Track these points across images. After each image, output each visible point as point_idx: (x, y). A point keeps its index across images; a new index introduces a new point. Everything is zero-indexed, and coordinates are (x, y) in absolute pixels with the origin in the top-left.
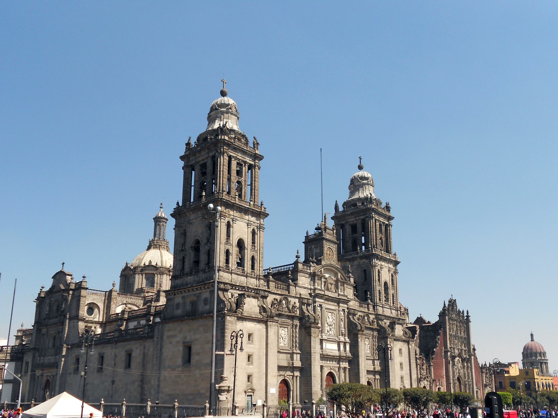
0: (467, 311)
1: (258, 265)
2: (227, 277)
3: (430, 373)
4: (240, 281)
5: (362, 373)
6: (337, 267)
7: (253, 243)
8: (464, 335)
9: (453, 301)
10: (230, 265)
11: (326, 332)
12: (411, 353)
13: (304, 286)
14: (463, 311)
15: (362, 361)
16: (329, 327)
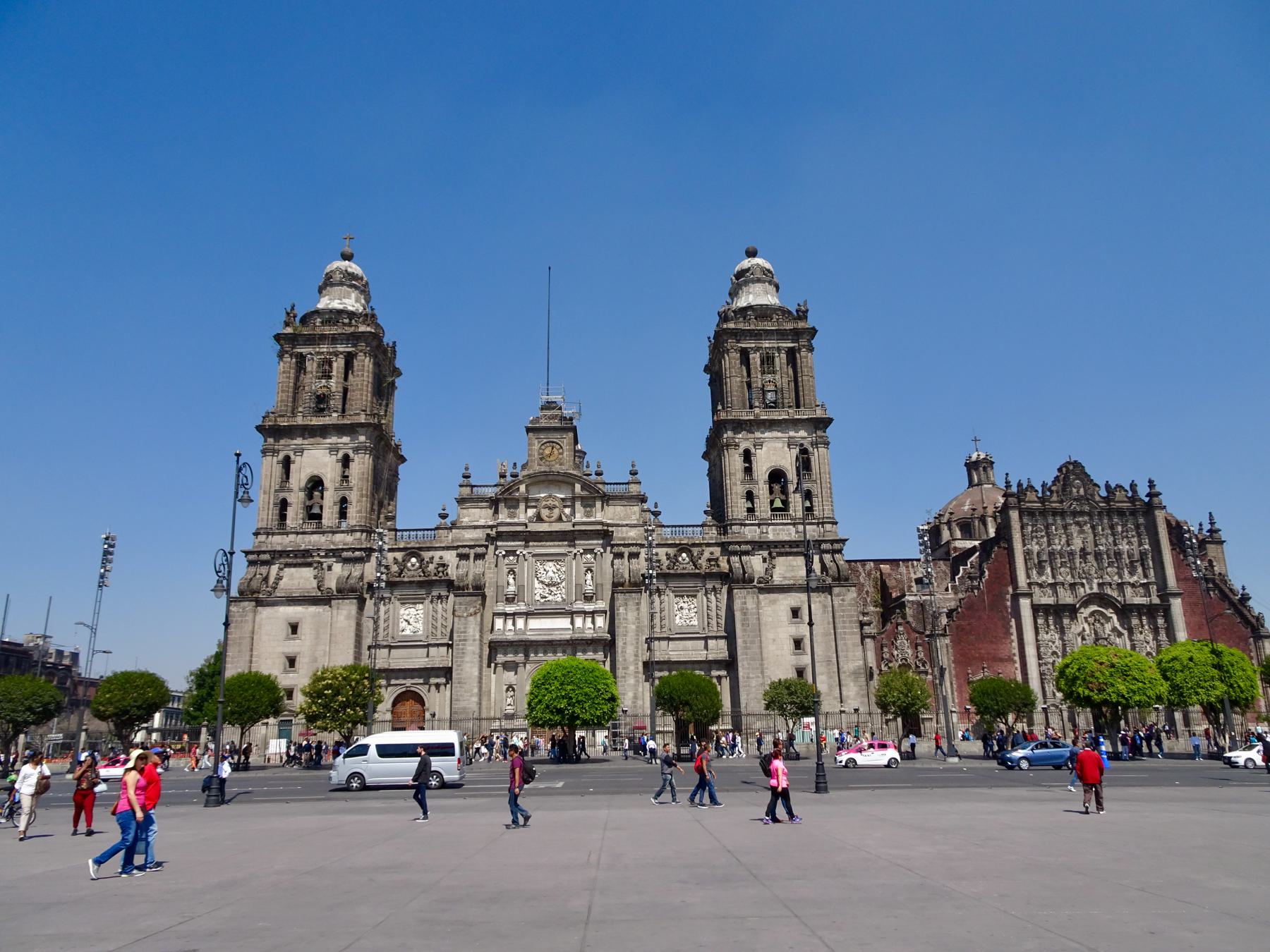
0: (1151, 482)
1: (355, 510)
2: (280, 542)
3: (932, 657)
4: (310, 542)
5: (626, 668)
6: (565, 473)
7: (345, 478)
8: (1140, 544)
9: (1071, 467)
10: (288, 522)
11: (538, 597)
12: (837, 614)
13: (476, 523)
14: (1133, 486)
15: (625, 643)
16: (547, 589)
